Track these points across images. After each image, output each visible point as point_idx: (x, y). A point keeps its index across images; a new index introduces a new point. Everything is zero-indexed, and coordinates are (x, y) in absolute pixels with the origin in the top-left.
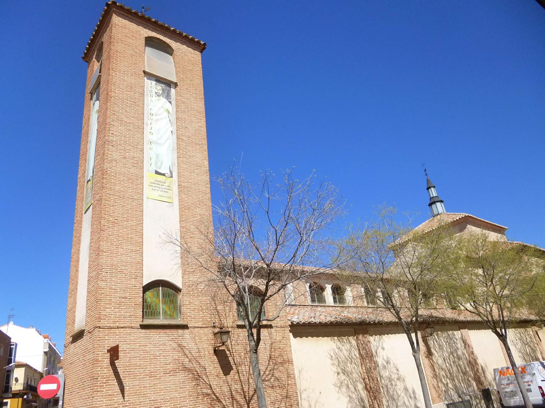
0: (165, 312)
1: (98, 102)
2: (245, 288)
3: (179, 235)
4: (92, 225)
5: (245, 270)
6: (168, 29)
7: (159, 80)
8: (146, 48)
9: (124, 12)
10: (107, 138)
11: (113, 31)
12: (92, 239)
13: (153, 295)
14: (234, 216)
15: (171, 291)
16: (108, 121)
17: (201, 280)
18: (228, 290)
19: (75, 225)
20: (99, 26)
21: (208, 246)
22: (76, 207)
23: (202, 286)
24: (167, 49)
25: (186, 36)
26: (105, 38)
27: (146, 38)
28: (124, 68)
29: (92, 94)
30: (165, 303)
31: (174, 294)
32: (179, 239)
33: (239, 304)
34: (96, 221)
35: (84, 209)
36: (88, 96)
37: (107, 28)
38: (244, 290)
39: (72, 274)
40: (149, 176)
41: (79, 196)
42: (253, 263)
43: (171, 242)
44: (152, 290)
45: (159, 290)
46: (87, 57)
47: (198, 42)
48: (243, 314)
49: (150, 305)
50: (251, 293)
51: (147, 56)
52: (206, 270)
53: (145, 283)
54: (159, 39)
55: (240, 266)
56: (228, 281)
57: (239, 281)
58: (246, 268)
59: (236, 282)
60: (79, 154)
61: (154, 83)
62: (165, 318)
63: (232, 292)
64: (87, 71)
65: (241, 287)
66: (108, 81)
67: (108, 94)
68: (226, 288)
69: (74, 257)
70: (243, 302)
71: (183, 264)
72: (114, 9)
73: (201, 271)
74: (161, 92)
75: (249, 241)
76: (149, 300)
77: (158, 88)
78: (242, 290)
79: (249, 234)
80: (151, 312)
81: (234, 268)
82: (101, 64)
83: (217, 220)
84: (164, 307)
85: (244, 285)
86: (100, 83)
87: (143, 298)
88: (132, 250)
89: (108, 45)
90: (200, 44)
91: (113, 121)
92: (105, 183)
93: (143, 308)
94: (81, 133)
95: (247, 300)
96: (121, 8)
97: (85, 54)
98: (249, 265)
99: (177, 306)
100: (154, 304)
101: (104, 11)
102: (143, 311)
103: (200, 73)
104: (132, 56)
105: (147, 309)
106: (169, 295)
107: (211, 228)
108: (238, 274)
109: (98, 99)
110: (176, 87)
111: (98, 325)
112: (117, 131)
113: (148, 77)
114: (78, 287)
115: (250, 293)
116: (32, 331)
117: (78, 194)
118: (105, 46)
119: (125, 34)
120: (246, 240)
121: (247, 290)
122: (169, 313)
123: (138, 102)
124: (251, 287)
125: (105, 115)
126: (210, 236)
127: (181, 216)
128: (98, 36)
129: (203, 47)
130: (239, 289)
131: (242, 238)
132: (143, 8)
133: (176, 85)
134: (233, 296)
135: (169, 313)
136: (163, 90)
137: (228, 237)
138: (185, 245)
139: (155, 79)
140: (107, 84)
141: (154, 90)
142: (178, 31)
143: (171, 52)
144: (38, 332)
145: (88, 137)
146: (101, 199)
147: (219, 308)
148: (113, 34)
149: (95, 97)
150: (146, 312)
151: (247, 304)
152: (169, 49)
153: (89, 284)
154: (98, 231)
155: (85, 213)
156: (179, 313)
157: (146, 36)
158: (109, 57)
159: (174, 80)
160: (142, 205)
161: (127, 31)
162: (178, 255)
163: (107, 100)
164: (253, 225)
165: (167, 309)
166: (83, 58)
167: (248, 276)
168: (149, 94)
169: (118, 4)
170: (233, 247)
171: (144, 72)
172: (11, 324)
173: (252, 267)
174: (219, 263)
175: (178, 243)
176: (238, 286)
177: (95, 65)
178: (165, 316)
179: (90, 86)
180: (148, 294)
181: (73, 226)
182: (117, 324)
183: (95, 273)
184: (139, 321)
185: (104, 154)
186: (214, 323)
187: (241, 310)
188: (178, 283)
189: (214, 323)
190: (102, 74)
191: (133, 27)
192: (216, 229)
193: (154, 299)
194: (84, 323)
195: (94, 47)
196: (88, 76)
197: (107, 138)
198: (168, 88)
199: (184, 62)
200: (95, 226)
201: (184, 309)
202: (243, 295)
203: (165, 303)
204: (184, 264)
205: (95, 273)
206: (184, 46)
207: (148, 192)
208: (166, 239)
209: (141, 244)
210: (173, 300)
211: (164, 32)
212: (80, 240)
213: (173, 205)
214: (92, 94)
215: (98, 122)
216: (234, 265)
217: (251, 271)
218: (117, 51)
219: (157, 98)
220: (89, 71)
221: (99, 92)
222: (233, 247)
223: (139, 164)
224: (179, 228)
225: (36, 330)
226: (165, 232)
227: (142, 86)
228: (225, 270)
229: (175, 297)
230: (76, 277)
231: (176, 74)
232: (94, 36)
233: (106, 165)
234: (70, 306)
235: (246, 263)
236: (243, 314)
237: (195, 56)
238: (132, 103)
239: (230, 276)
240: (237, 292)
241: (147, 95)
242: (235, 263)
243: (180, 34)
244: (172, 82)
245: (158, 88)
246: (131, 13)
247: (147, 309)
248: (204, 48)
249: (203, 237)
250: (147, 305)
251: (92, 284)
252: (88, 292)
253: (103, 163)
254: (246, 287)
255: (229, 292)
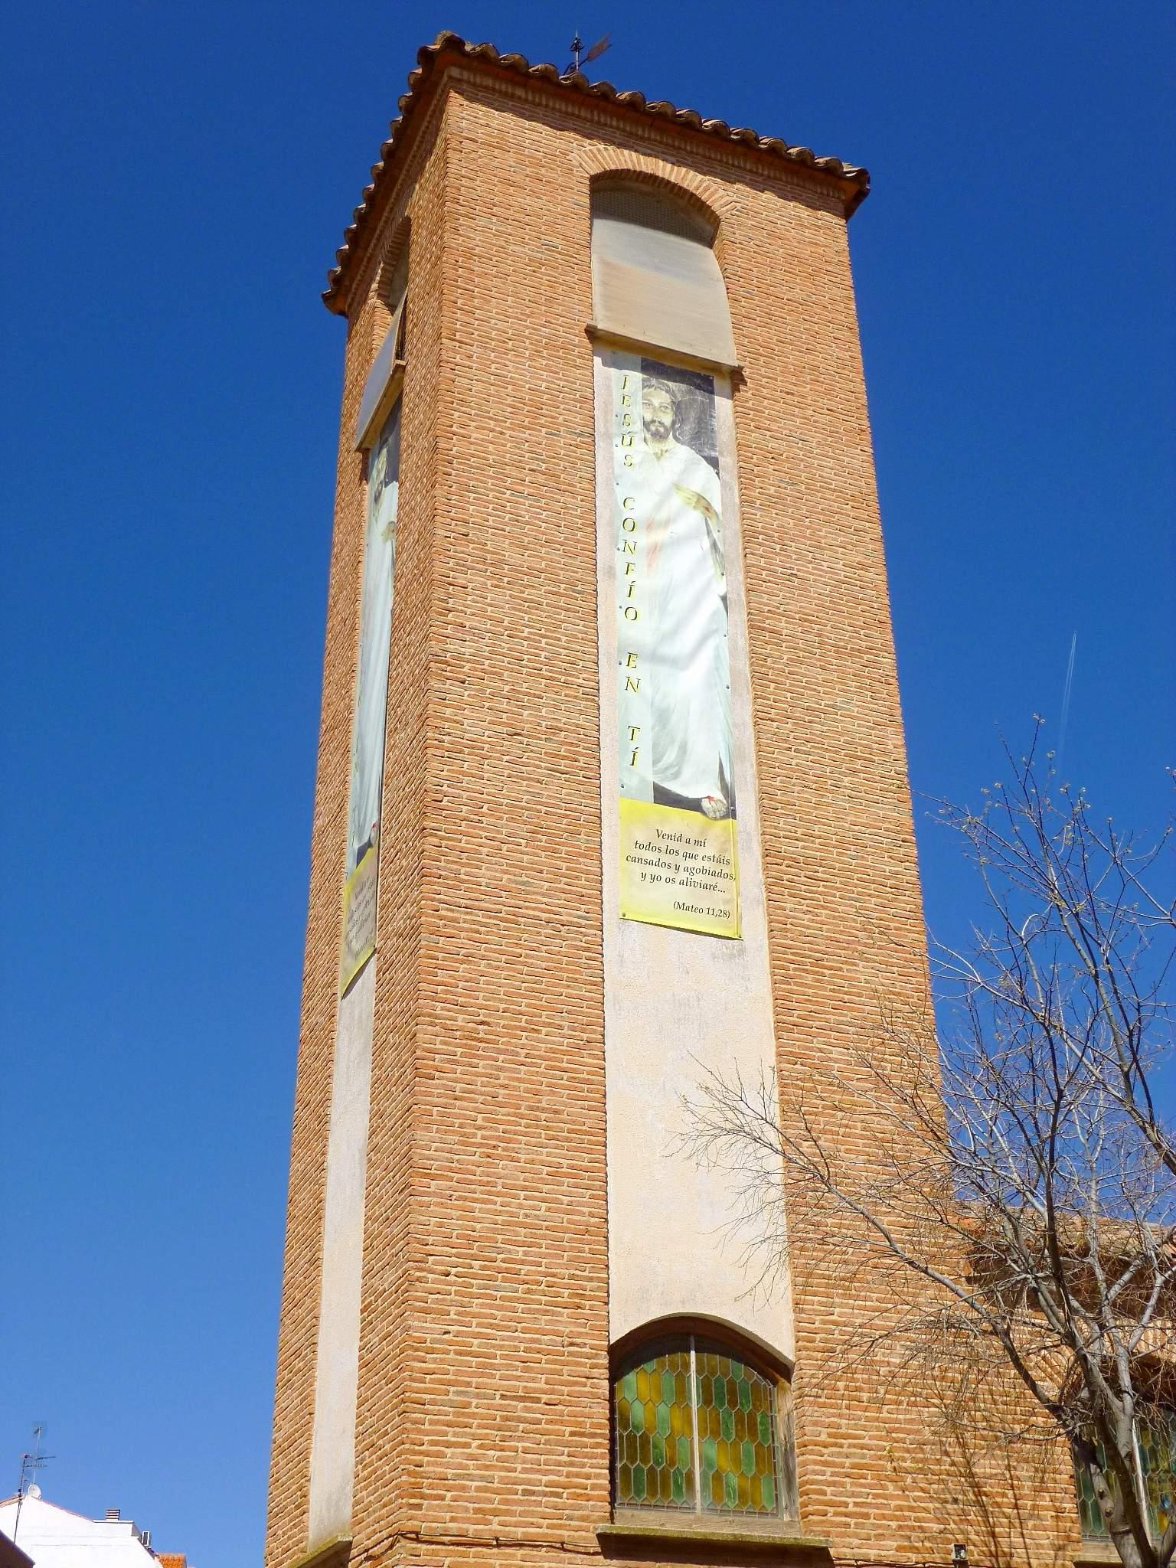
0: (718, 1477)
1: (396, 484)
2: (1115, 1369)
3: (776, 1097)
4: (378, 1050)
5: (1114, 1275)
6: (688, 129)
7: (657, 363)
8: (597, 222)
9: (496, 77)
10: (435, 646)
11: (453, 168)
12: (377, 1115)
13: (660, 1393)
14: (1049, 1001)
15: (741, 1372)
16: (440, 568)
17: (892, 1320)
18: (1026, 1377)
19: (305, 1050)
20: (390, 155)
21: (921, 1150)
22: (307, 967)
23: (892, 1355)
24: (691, 220)
25: (773, 150)
26: (419, 202)
27: (595, 180)
28: (501, 325)
29: (366, 452)
30: (715, 1434)
31: (756, 1384)
32: (775, 1111)
33: (1085, 1454)
34: (394, 1029)
35: (340, 975)
36: (349, 460)
37: (425, 160)
38: (1113, 1381)
39: (292, 1275)
40: (625, 816)
41: (318, 918)
42: (1153, 1239)
43: (739, 1130)
44: (652, 1366)
45: (686, 1366)
46: (343, 298)
47: (832, 171)
48: (1108, 1504)
49: (645, 1439)
50: (1149, 1398)
51: (605, 264)
52: (910, 1272)
53: (619, 1330)
54: (652, 179)
55: (1085, 1251)
56: (1027, 1328)
57: (1084, 1329)
58: (1116, 1267)
59: (1070, 1339)
60: (317, 723)
61: (636, 377)
62: (717, 1506)
63: (1051, 1390)
64: (343, 354)
65: (1094, 1362)
66: (435, 388)
67: (435, 449)
68: (1018, 1365)
69: (303, 1198)
70: (1110, 1440)
71: (796, 1241)
72: (455, 72)
73: (889, 1274)
74: (667, 419)
75: (1127, 1125)
76: (638, 1413)
77: (656, 402)
78: (1100, 1378)
79: (1129, 1089)
80: (652, 1470)
81: (1058, 1266)
82: (404, 318)
83: (959, 1017)
84: (712, 1451)
85: (1108, 1351)
86: (398, 404)
87: (611, 1399)
88: (556, 1173)
89: (432, 233)
90: (841, 176)
91: (463, 567)
92: (432, 851)
93: (612, 1452)
94: (323, 631)
95: (1129, 1438)
96: (484, 61)
97: (337, 281)
98: (1133, 1247)
99: (772, 1451)
100: (659, 1437)
101: (413, 88)
102: (612, 1469)
103: (848, 312)
104: (535, 264)
105: (632, 1459)
106: (732, 1392)
107: (932, 1066)
108: (1076, 1292)
109: (393, 475)
110: (735, 389)
111: (410, 1525)
112: (480, 612)
113: (608, 352)
114: (321, 1339)
115: (1144, 1396)
116: (119, 1536)
117: (317, 906)
118: (419, 237)
119: (507, 176)
120: (1107, 1118)
121: (1126, 1381)
122: (734, 1480)
123: (568, 479)
124: (1146, 1366)
125: (425, 539)
126: (929, 1101)
127: (782, 1003)
128: (387, 197)
129: (853, 189)
130: (1088, 1371)
131: (1089, 1107)
132: (577, 48)
133: (736, 377)
134: (1055, 1410)
135: (734, 1480)
136: (677, 407)
137: (1022, 1105)
138: (806, 1147)
139: (637, 359)
140: (432, 405)
141: (639, 412)
142: (735, 132)
143: (708, 228)
144: (143, 1541)
145: (352, 647)
146: (416, 930)
147: (984, 1467)
148: (450, 180)
149: (380, 465)
150: (625, 1470)
151: (1130, 1456)
152: (699, 221)
153: (366, 1326)
154: (400, 1075)
155: (344, 997)
156: (782, 1487)
157: (595, 170)
158: (436, 284)
159: (727, 355)
160: (596, 949)
161: (511, 159)
162: (775, 1193)
163: (432, 475)
164: (1145, 1046)
165: (724, 1462)
166: (326, 298)
167: (1129, 1309)
168: (614, 430)
169: (468, 48)
170: (1045, 1155)
171: (592, 333)
172: (32, 1501)
173: (1147, 1259)
174: (979, 1234)
175: (772, 1136)
176: (1082, 1359)
177: (379, 325)
178: (717, 1497)
179: (358, 415)
180: (635, 1382)
181: (294, 1055)
182: (495, 1526)
183: (390, 1276)
184: (592, 1516)
185: (423, 720)
186: (959, 1548)
187: (1099, 1484)
188: (778, 1334)
189: (959, 1548)
190: (409, 362)
191: (535, 137)
192: (958, 1066)
193: (663, 1409)
194: (348, 1511)
195: (375, 249)
196: (350, 377)
197: (435, 646)
198: (700, 396)
199: (773, 273)
200: (390, 1056)
201: (808, 1467)
202: (1108, 1407)
203: (713, 1430)
204: (805, 1243)
205: (390, 1276)
206: (768, 196)
207: (626, 891)
208: (716, 1118)
209: (596, 1138)
210: (752, 1417)
211: (674, 144)
212: (323, 1120)
213: (742, 952)
214: (366, 452)
215: (397, 578)
216: (1055, 1251)
217: (1141, 1279)
218: (470, 254)
219: (654, 447)
220: (353, 352)
221: (398, 439)
222: (1045, 1155)
223: (581, 760)
224: (772, 1060)
225: (135, 1531)
226: (712, 1084)
227: (583, 399)
228: (1007, 1273)
229: (764, 1403)
230: (312, 1290)
231: (737, 326)
232: (371, 199)
233: (437, 771)
234: (287, 1427)
235: (1116, 1236)
236: (1108, 1504)
237: (816, 235)
238: (541, 479)
239: (1034, 1304)
240: (1076, 1387)
241: (609, 437)
242: (1063, 1240)
243: (747, 144)
244: (716, 367)
245: (656, 402)
246: (528, 75)
247: (632, 1459)
248: (861, 195)
249: (891, 1104)
250: (631, 1439)
251: (383, 1327)
252: (364, 1365)
253: (421, 763)
254: (1123, 1367)
255: (1033, 1386)
